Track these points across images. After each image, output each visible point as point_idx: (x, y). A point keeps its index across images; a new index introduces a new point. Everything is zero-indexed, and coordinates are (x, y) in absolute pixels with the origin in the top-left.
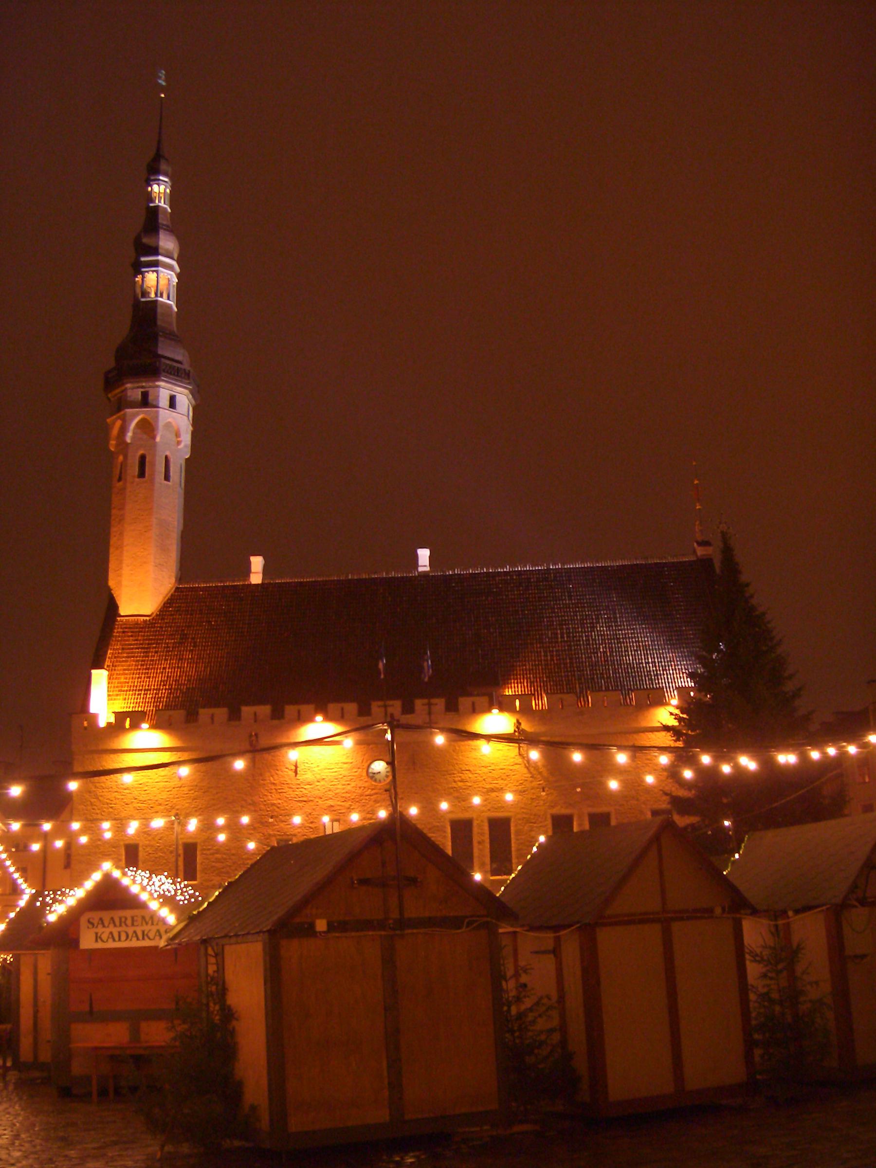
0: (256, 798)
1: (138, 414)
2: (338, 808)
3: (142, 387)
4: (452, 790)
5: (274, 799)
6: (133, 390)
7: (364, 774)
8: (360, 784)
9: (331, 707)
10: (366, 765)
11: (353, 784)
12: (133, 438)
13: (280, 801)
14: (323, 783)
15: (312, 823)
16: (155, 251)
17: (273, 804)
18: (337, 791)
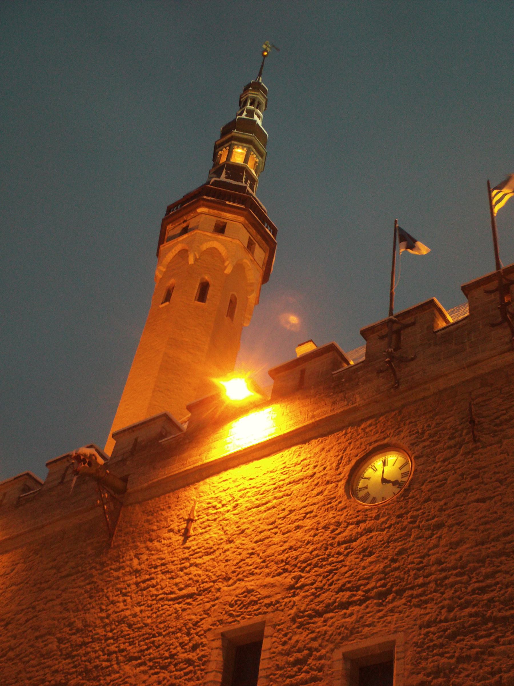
1: (172, 247)
2: (264, 592)
5: (128, 607)
11: (308, 523)
13: (137, 609)
15: (194, 648)
17: (121, 621)
18: (269, 551)
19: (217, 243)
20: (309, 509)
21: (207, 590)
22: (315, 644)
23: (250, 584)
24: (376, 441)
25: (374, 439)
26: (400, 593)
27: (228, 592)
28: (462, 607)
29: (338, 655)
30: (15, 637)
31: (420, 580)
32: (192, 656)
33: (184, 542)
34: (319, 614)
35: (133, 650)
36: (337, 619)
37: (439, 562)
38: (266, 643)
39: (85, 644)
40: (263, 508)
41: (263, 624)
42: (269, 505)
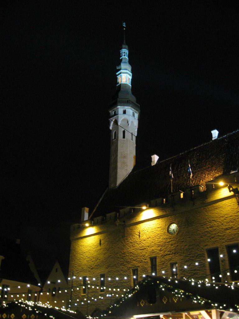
0: (125, 251)
2: (156, 250)
3: (114, 110)
4: (206, 233)
5: (131, 250)
6: (112, 112)
7: (166, 232)
8: (165, 237)
9: (152, 201)
10: (167, 227)
11: (162, 237)
12: (112, 128)
13: (133, 251)
14: (150, 239)
15: (145, 259)
16: (120, 70)
17: (131, 253)
18: (155, 242)
19: (125, 116)
20: (161, 234)
21: (145, 249)
22: (165, 261)
23: (153, 248)
24: (172, 221)
25: (171, 221)
26: (178, 253)
27: (150, 249)
28: (187, 257)
29: (169, 263)
30: (110, 253)
31: (181, 251)
32: (145, 261)
33: (139, 237)
34: (165, 256)
35: (135, 259)
36: (168, 257)
37: (183, 249)
38: (157, 260)
39: (125, 256)
40: (153, 232)
41: (156, 256)
42: (154, 232)
